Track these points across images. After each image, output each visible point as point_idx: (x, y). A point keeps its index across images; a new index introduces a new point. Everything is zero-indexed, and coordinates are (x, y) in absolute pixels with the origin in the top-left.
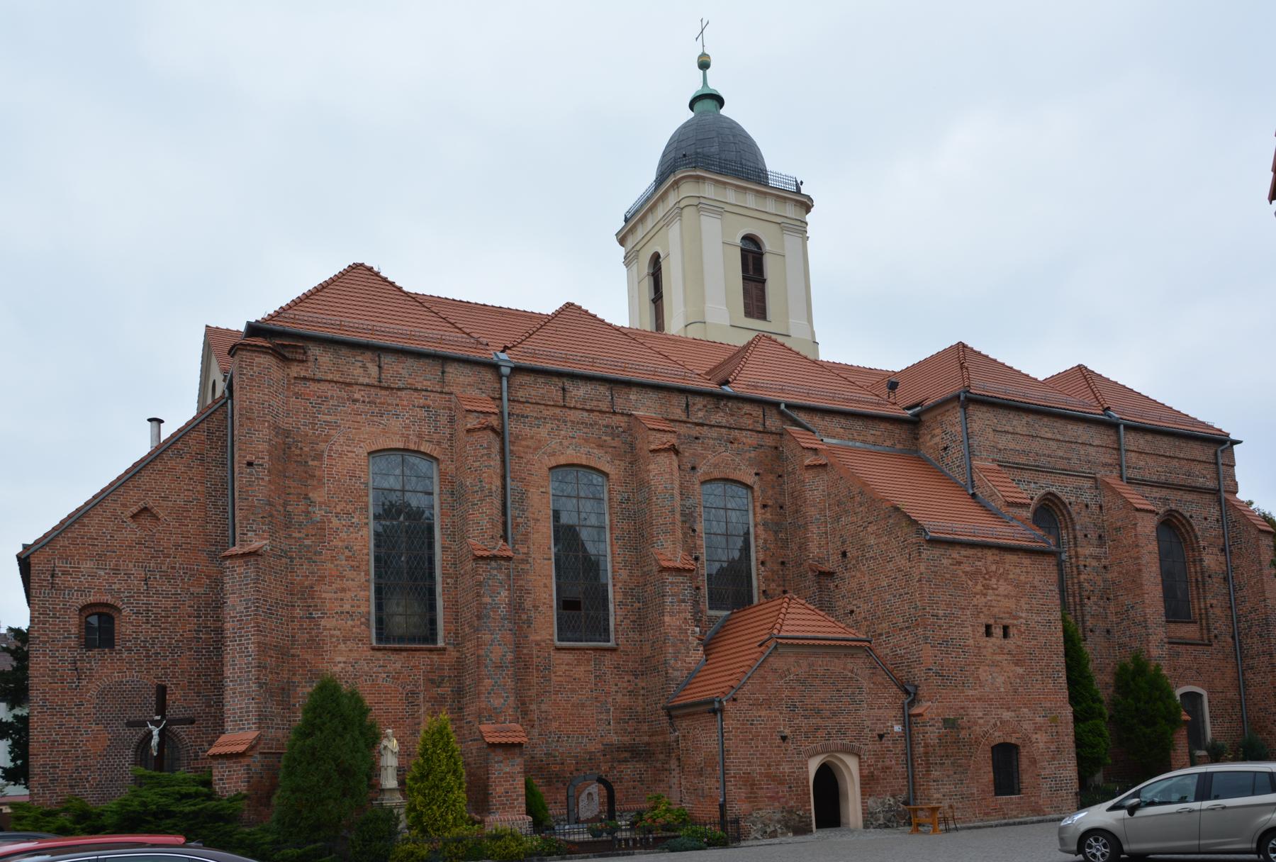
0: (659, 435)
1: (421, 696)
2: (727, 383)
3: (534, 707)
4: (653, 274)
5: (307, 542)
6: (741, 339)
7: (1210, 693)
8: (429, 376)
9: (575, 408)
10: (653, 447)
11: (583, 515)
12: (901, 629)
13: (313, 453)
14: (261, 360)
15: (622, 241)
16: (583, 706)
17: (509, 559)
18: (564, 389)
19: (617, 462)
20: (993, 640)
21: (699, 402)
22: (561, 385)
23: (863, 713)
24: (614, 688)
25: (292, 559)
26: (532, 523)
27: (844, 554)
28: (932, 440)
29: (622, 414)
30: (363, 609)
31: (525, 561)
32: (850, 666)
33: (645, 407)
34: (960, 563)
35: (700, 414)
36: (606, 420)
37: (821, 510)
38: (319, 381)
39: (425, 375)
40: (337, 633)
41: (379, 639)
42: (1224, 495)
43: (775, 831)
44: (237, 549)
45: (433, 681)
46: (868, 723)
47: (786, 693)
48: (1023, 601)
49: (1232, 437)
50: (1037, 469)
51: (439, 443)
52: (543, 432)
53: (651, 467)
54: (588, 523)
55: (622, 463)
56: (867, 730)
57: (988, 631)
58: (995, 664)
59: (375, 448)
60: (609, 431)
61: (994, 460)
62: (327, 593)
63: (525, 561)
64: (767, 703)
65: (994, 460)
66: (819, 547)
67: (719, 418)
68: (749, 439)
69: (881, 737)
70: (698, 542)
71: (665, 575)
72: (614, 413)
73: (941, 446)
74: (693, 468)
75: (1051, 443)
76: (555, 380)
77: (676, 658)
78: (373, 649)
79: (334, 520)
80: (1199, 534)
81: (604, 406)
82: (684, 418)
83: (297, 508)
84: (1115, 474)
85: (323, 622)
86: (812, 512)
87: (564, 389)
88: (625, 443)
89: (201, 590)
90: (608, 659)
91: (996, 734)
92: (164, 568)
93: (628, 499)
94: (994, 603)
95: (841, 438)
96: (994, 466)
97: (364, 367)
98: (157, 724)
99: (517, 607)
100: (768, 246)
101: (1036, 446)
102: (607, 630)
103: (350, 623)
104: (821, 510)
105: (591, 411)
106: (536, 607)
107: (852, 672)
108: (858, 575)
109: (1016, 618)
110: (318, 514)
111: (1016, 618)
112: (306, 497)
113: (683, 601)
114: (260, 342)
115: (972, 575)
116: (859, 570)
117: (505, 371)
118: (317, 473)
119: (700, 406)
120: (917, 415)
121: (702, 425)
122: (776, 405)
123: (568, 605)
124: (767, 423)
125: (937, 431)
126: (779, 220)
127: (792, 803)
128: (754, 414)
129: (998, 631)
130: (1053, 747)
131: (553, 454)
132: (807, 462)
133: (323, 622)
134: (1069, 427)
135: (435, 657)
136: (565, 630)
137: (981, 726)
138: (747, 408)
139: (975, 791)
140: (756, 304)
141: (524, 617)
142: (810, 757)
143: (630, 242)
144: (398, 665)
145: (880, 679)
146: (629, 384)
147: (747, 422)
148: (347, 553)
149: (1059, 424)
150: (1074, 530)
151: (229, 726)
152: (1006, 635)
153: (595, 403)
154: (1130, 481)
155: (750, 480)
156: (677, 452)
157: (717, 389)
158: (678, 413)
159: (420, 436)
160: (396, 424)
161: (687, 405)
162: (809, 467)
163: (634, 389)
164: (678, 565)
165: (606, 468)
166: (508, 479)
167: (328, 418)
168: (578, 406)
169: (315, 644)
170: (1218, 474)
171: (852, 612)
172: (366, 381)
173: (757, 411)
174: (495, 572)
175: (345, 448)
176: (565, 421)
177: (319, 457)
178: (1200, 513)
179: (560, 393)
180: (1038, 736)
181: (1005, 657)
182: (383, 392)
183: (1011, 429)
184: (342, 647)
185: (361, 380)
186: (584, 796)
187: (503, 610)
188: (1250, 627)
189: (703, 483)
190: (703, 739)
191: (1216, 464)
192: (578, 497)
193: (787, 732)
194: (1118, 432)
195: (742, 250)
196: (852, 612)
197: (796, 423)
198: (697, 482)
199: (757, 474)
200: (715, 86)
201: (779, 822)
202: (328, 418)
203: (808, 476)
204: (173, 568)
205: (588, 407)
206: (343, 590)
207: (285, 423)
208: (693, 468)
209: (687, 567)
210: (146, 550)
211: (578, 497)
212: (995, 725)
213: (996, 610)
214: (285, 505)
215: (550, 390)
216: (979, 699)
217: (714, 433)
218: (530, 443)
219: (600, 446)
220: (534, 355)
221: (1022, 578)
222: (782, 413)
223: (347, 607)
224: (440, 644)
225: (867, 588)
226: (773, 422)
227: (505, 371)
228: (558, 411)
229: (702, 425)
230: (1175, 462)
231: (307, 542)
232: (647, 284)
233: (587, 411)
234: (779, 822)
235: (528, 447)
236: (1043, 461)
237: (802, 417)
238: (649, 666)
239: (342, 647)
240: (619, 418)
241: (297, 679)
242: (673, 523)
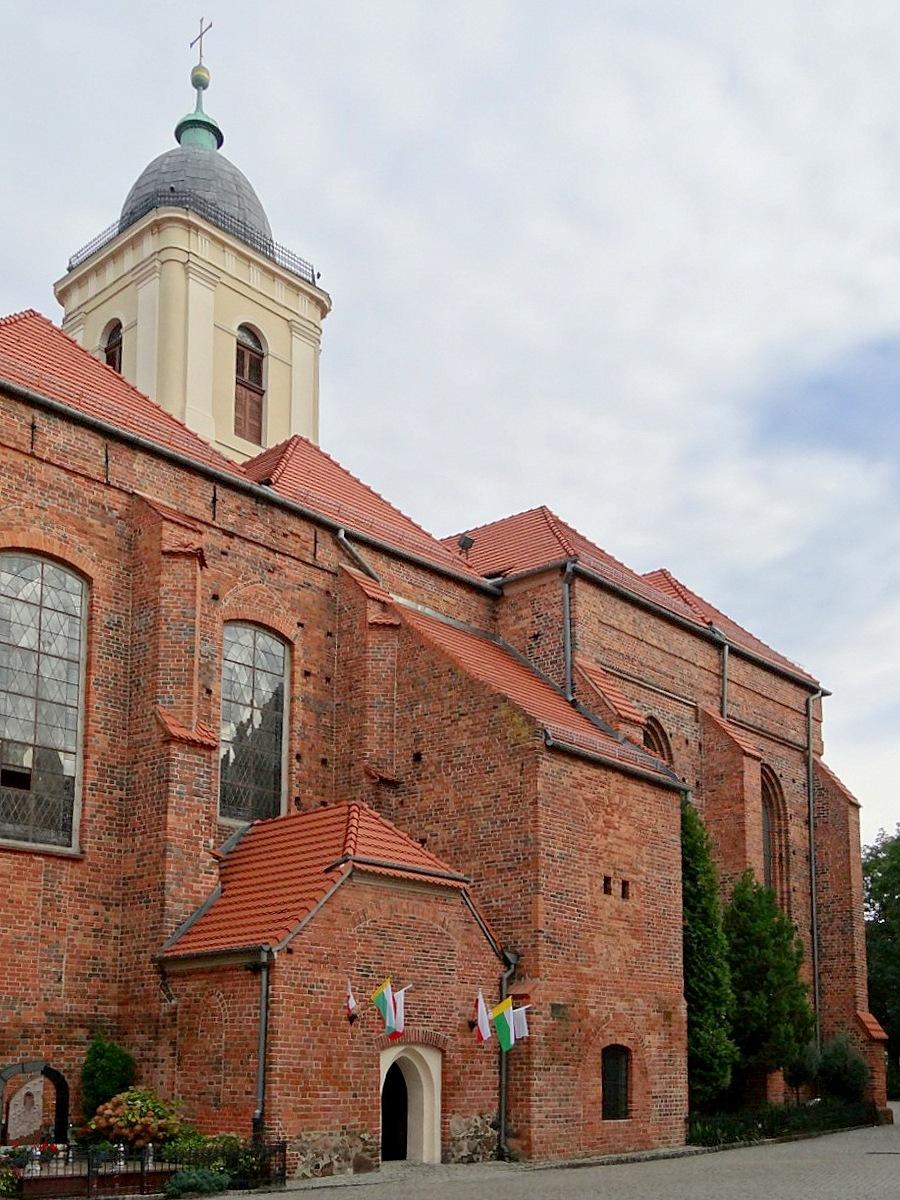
0: (178, 531)
2: (268, 483)
9: (48, 462)
10: (166, 548)
11: (45, 636)
12: (501, 871)
16: (21, 947)
18: (33, 427)
19: (106, 563)
20: (611, 898)
21: (229, 501)
22: (29, 419)
27: (417, 757)
28: (517, 624)
29: (120, 490)
33: (156, 485)
35: (231, 518)
36: (95, 493)
37: (387, 691)
50: (640, 684)
53: (164, 578)
54: (53, 650)
55: (114, 567)
61: (597, 661)
65: (597, 661)
66: (380, 746)
67: (256, 530)
68: (296, 572)
71: (174, 747)
72: (108, 485)
73: (530, 633)
74: (215, 597)
75: (655, 652)
76: (21, 408)
77: (179, 882)
81: (94, 471)
82: (208, 517)
86: (373, 689)
87: (33, 427)
88: (121, 536)
90: (68, 874)
93: (119, 624)
95: (409, 598)
96: (597, 668)
101: (641, 652)
104: (387, 691)
105: (74, 473)
108: (438, 788)
111: (637, 872)
116: (440, 782)
119: (232, 505)
120: (500, 587)
121: (231, 535)
122: (333, 530)
124: (318, 555)
128: (303, 535)
129: (617, 888)
132: (371, 618)
134: (675, 636)
138: (295, 525)
146: (134, 445)
147: (291, 545)
149: (666, 629)
153: (81, 463)
155: (292, 632)
156: (203, 564)
158: (199, 508)
161: (215, 500)
162: (375, 626)
163: (141, 456)
165: (89, 569)
168: (54, 460)
173: (305, 531)
176: (31, 480)
179: (27, 432)
186: (19, 1097)
189: (228, 622)
190: (229, 1010)
192: (41, 606)
197: (355, 561)
198: (219, 619)
199: (300, 625)
200: (210, 114)
205: (71, 467)
208: (215, 597)
209: (207, 741)
211: (41, 606)
217: (247, 550)
219: (82, 532)
222: (338, 543)
225: (452, 807)
226: (328, 555)
228: (21, 459)
229: (231, 535)
233: (67, 471)
236: (646, 674)
237: (363, 555)
238: (137, 889)
240: (113, 493)
242: (190, 670)
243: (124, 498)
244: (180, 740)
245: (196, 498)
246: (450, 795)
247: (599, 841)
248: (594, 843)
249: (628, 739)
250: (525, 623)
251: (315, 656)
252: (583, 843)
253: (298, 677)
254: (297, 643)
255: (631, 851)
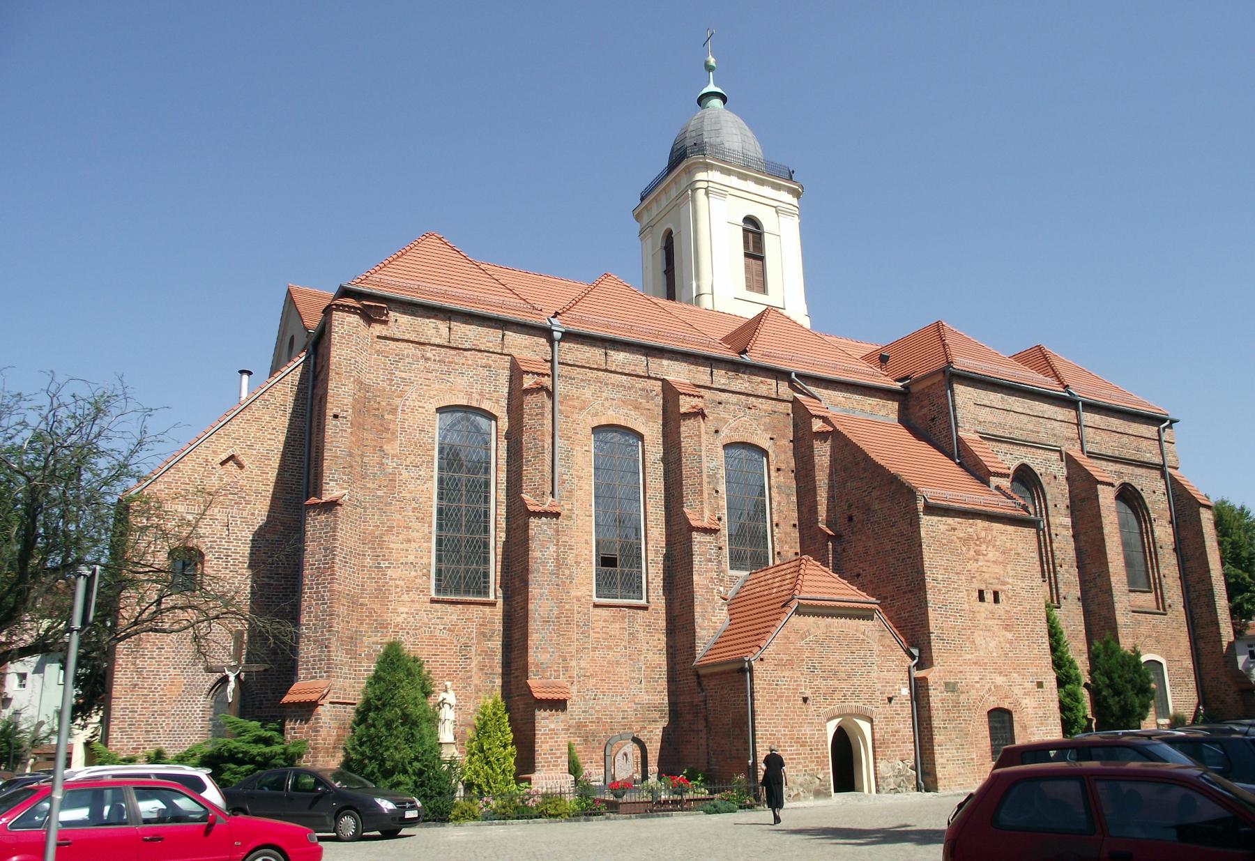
0: (688, 399)
1: (473, 649)
2: (745, 352)
3: (573, 663)
4: (665, 248)
5: (380, 493)
6: (750, 312)
7: (1168, 661)
8: (491, 338)
13: (389, 408)
14: (351, 320)
15: (638, 217)
17: (557, 515)
23: (874, 675)
24: (645, 647)
25: (365, 508)
26: (576, 480)
27: (850, 519)
30: (425, 561)
31: (569, 517)
32: (862, 628)
34: (954, 529)
38: (397, 340)
39: (487, 337)
40: (401, 583)
41: (438, 591)
42: (1169, 470)
43: (798, 794)
44: (313, 500)
45: (484, 634)
46: (878, 686)
47: (807, 654)
48: (1009, 567)
49: (1171, 417)
51: (497, 401)
52: (588, 393)
56: (878, 693)
57: (981, 598)
58: (988, 629)
59: (442, 404)
60: (644, 393)
62: (395, 543)
63: (569, 517)
64: (790, 664)
69: (890, 700)
70: (721, 503)
71: (694, 534)
72: (649, 377)
74: (717, 432)
78: (433, 601)
79: (404, 472)
80: (1149, 506)
83: (372, 459)
84: (1078, 446)
85: (389, 572)
89: (275, 537)
91: (992, 699)
92: (245, 514)
94: (985, 569)
97: (436, 328)
98: (231, 668)
99: (560, 563)
100: (766, 226)
102: (640, 587)
103: (413, 573)
106: (577, 563)
107: (864, 634)
109: (1004, 583)
110: (390, 464)
112: (381, 450)
113: (710, 560)
114: (350, 302)
115: (966, 541)
117: (557, 335)
118: (391, 426)
123: (606, 561)
125: (926, 402)
126: (775, 204)
127: (813, 766)
130: (1040, 713)
131: (596, 415)
132: (815, 429)
133: (389, 572)
135: (487, 609)
136: (604, 585)
137: (978, 690)
139: (974, 756)
140: (758, 281)
141: (567, 572)
142: (829, 720)
143: (645, 219)
144: (454, 617)
145: (887, 641)
148: (414, 505)
150: (1045, 500)
151: (302, 673)
152: (996, 600)
154: (1091, 455)
157: (736, 357)
159: (481, 394)
160: (462, 382)
164: (705, 524)
165: (641, 430)
166: (557, 438)
167: (403, 375)
169: (381, 593)
170: (1162, 450)
171: (858, 575)
172: (438, 341)
174: (545, 527)
175: (417, 404)
177: (394, 411)
178: (1153, 490)
179: (603, 357)
180: (1026, 701)
181: (996, 622)
182: (452, 352)
183: (988, 403)
184: (405, 597)
185: (434, 341)
187: (551, 566)
188: (1198, 597)
191: (1160, 440)
193: (808, 693)
194: (1077, 409)
195: (744, 230)
196: (858, 575)
201: (801, 785)
202: (403, 375)
203: (816, 444)
204: (253, 514)
206: (409, 541)
207: (368, 378)
208: (717, 432)
209: (714, 527)
210: (230, 497)
212: (990, 689)
213: (987, 576)
214: (362, 456)
215: (593, 355)
216: (975, 663)
218: (576, 403)
219: (636, 408)
220: (580, 321)
221: (1008, 545)
223: (411, 558)
224: (492, 598)
226: (784, 390)
227: (557, 335)
228: (601, 373)
230: (1125, 439)
231: (380, 493)
232: (661, 256)
234: (801, 785)
235: (575, 407)
239: (405, 597)
241: (364, 628)
242: (701, 484)
243: (660, 383)
244: (698, 529)
245: (702, 374)
246: (871, 543)
247: (972, 566)
248: (969, 567)
249: (998, 488)
250: (925, 410)
251: (783, 457)
252: (959, 568)
253: (773, 473)
254: (770, 452)
255: (998, 569)
